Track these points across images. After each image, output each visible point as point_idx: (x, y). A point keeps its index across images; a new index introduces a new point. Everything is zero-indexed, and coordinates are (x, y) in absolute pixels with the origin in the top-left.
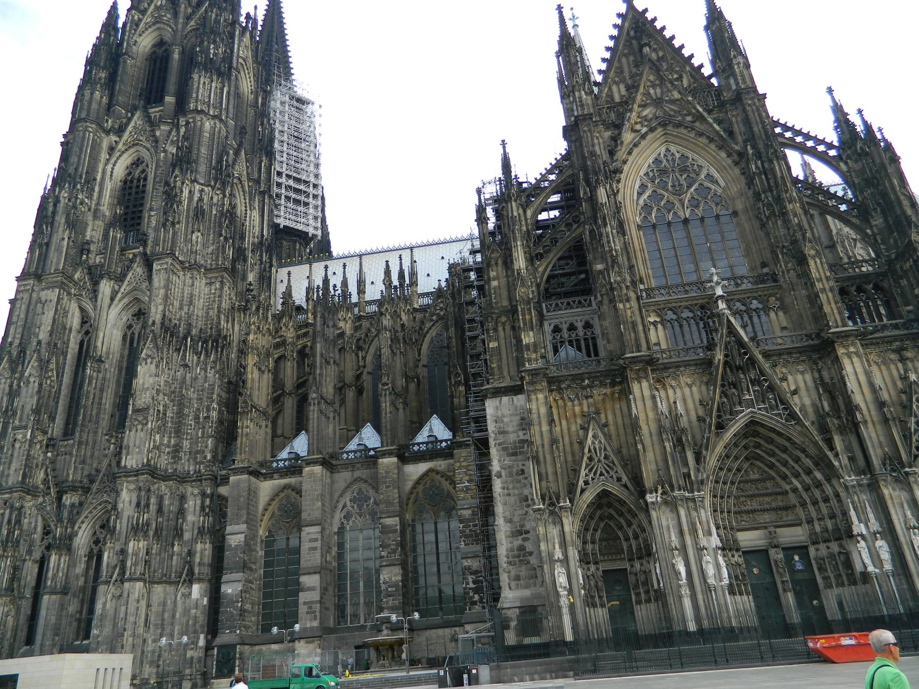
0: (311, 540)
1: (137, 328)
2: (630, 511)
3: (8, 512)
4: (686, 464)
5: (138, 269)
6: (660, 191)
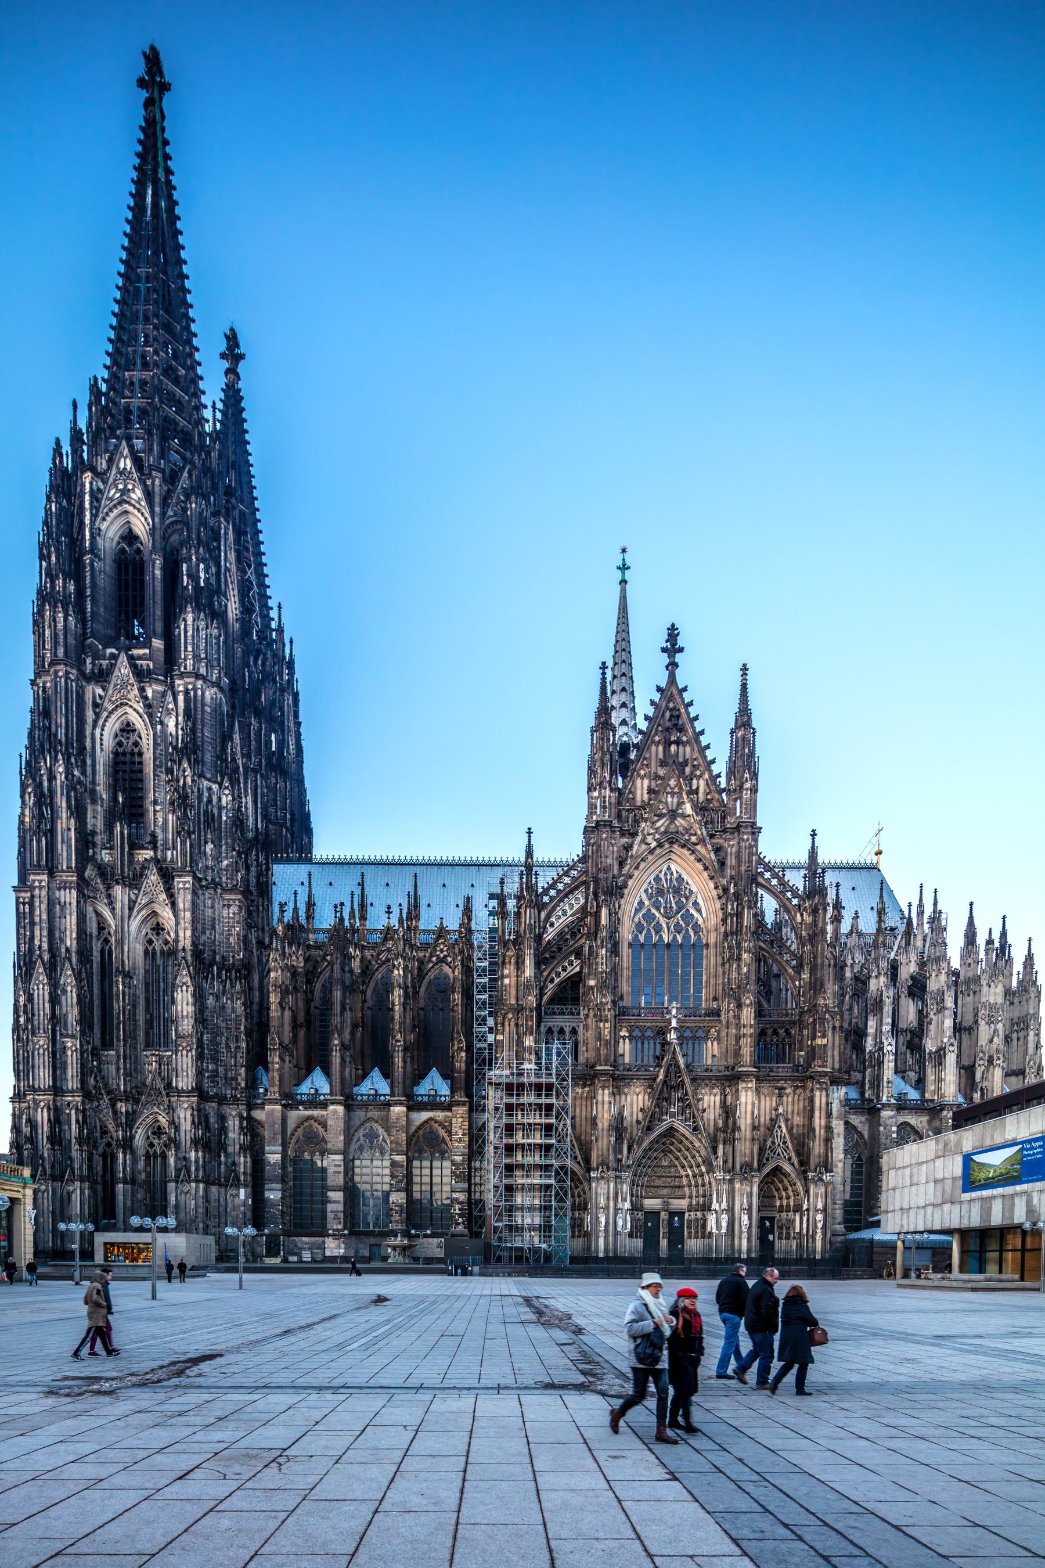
0: (335, 1166)
1: (158, 945)
2: (579, 1179)
3: (73, 1112)
4: (621, 1152)
5: (153, 877)
6: (654, 911)
